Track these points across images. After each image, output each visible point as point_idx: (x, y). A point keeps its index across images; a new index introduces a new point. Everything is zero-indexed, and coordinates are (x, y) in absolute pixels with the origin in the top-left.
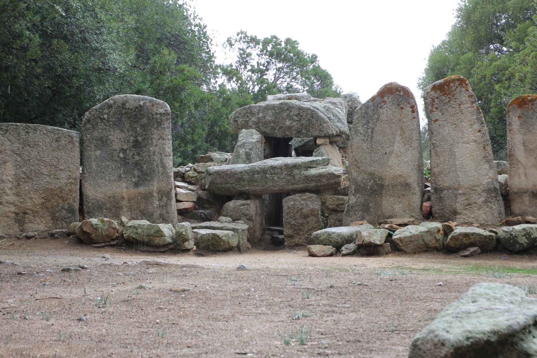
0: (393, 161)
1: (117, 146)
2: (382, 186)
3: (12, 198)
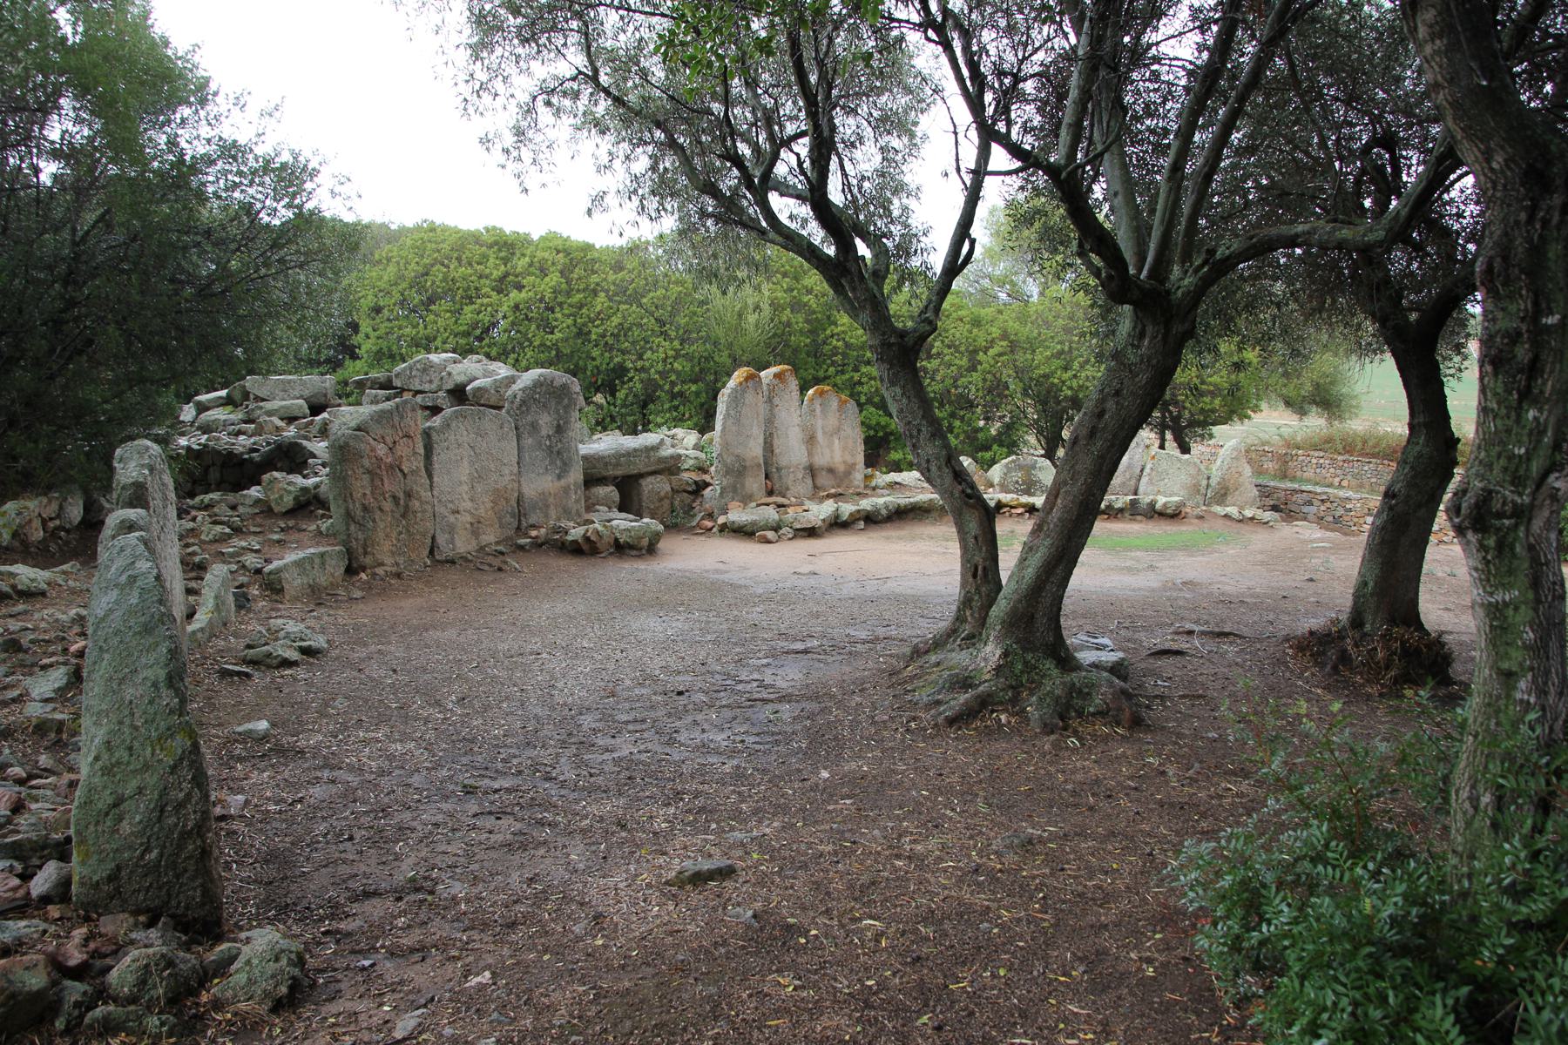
0: (752, 443)
1: (544, 432)
2: (745, 467)
3: (468, 505)
